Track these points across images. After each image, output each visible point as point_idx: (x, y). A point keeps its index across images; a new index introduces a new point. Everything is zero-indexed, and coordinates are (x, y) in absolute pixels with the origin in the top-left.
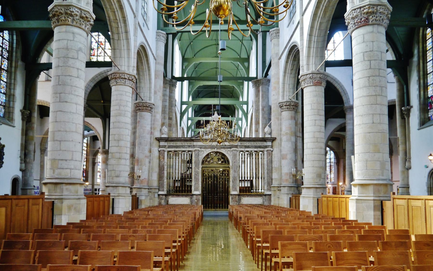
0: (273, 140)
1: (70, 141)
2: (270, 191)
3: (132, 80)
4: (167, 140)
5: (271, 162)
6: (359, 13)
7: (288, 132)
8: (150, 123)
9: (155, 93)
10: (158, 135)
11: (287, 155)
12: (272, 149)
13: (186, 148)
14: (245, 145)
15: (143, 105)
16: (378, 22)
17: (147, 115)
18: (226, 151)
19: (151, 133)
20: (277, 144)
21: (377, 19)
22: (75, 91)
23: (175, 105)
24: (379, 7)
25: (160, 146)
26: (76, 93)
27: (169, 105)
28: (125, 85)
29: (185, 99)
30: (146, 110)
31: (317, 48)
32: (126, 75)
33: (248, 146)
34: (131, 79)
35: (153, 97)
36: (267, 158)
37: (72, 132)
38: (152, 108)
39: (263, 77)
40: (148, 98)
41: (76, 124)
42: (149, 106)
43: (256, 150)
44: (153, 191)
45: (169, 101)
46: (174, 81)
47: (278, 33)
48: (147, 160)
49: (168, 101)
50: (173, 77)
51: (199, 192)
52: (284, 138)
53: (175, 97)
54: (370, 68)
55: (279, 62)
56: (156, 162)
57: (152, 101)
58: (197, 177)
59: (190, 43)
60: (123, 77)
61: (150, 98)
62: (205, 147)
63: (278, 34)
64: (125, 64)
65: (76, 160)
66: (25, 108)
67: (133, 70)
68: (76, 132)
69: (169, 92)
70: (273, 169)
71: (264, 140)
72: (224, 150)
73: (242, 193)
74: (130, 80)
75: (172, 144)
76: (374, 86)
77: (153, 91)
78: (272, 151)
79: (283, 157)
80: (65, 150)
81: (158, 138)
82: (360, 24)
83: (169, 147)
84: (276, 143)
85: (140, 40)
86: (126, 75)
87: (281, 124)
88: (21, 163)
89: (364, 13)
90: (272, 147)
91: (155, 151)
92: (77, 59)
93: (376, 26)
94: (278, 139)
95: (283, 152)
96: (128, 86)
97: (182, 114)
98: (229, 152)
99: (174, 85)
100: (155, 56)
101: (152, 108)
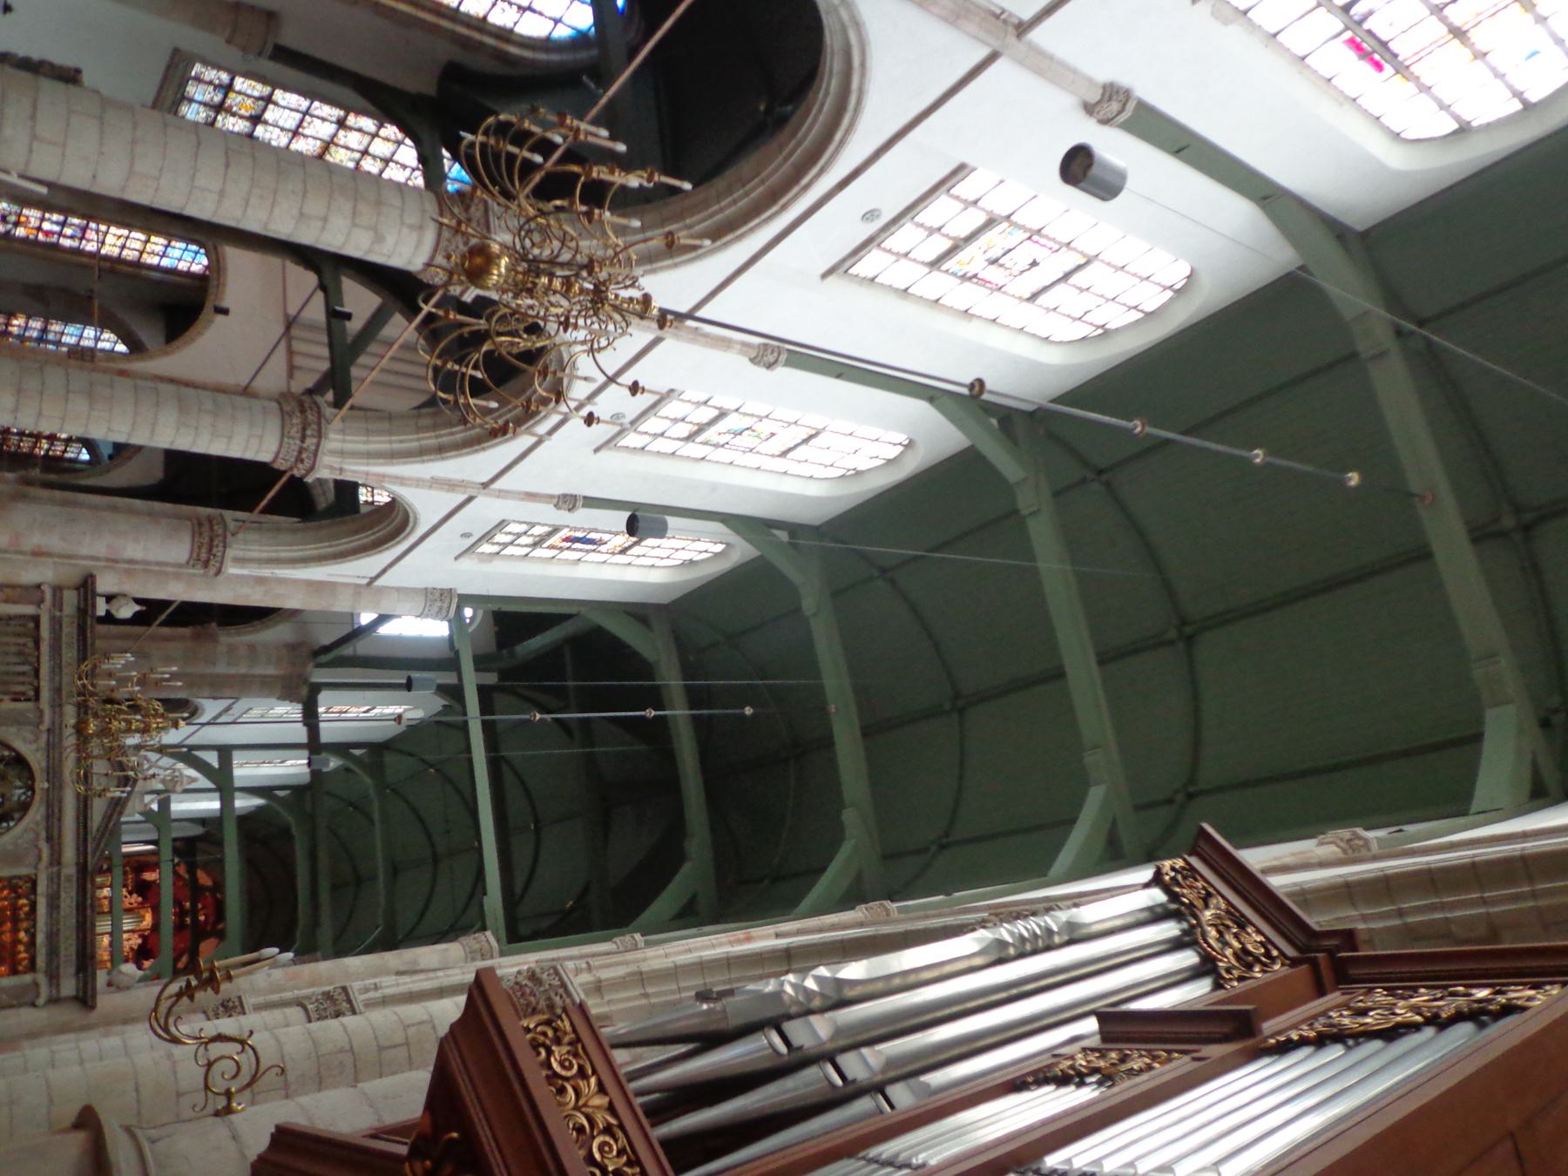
1: (101, 144)
3: (299, 460)
4: (84, 611)
6: (547, 987)
8: (151, 556)
9: (261, 581)
10: (105, 584)
13: (52, 680)
14: (63, 895)
15: (218, 536)
18: (37, 824)
19: (112, 562)
22: (262, 197)
23: (215, 695)
25: (58, 590)
26: (253, 201)
27: (218, 676)
28: (283, 436)
30: (196, 548)
32: (315, 441)
33: (58, 907)
34: (304, 456)
35: (245, 572)
37: (132, 164)
38: (206, 564)
40: (241, 554)
41: (158, 179)
42: (215, 556)
43: (40, 938)
45: (233, 676)
46: (304, 691)
49: (233, 671)
50: (316, 689)
53: (248, 696)
59: (432, 766)
60: (309, 432)
61: (240, 561)
62: (53, 748)
63: (479, 956)
64: (350, 442)
65: (31, 151)
67: (331, 468)
68: (131, 173)
69: (265, 676)
72: (38, 817)
74: (300, 452)
76: (319, 1073)
77: (266, 572)
78: (33, 1005)
80: (68, 125)
81: (93, 583)
82: (519, 994)
83: (56, 624)
84: (69, 1013)
85: (426, 505)
86: (315, 441)
89: (549, 999)
92: (354, 225)
96: (281, 446)
98: (31, 835)
99: (287, 695)
101: (206, 564)
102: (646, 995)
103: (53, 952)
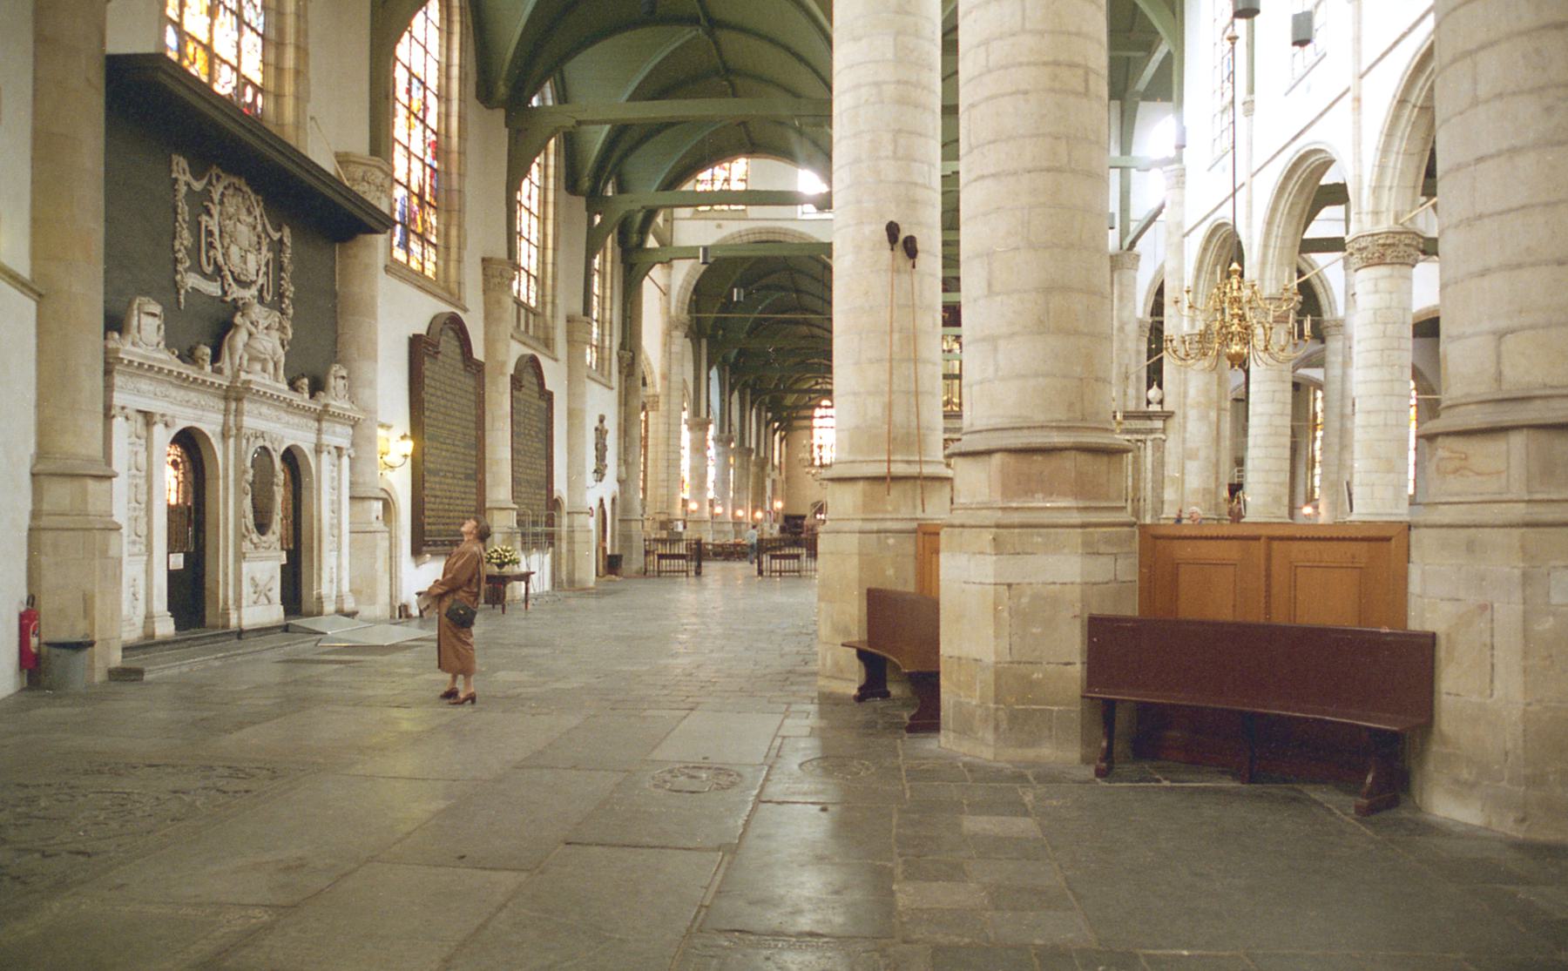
0: (1167, 416)
5: (1162, 464)
7: (1202, 399)
11: (1198, 449)
12: (1163, 437)
16: (1399, 261)
20: (1177, 425)
21: (1400, 255)
24: (1403, 236)
31: (1282, 248)
36: (1153, 455)
39: (1121, 248)
47: (1183, 175)
52: (1193, 414)
54: (1384, 336)
55: (1182, 242)
66: (623, 346)
70: (1166, 480)
71: (1149, 416)
78: (1164, 441)
79: (1188, 455)
84: (1173, 423)
87: (1185, 382)
88: (619, 466)
90: (1164, 431)
93: (1398, 266)
94: (1176, 411)
95: (1190, 445)
102: (1391, 188)
103: (1137, 431)
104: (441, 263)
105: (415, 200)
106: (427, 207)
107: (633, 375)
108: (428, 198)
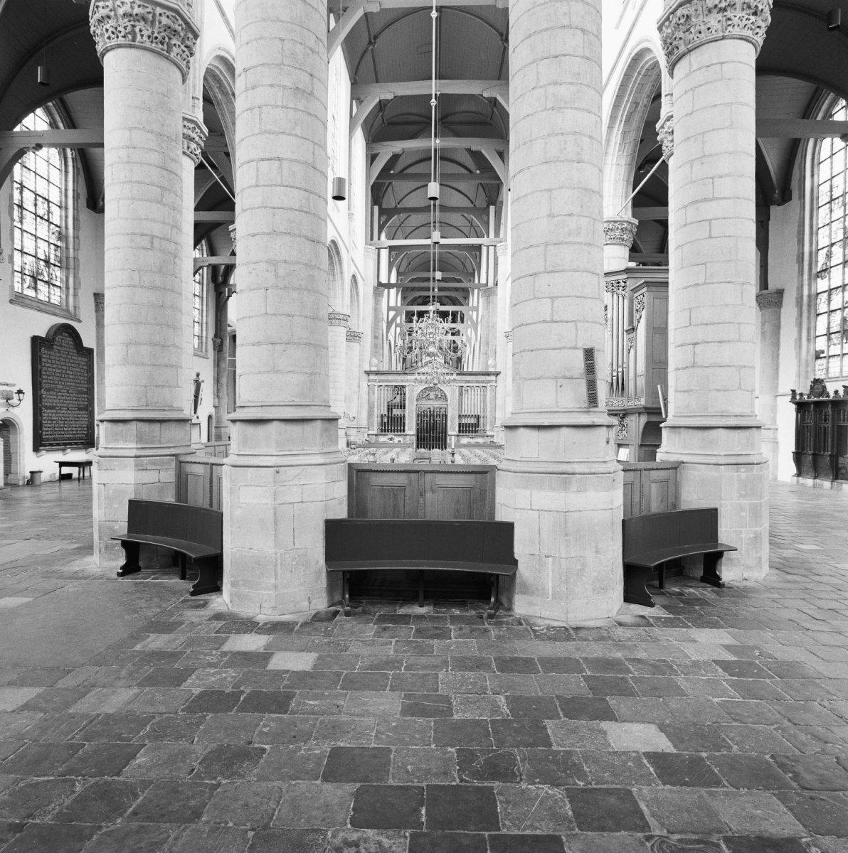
0: (497, 374)
2: (493, 431)
4: (377, 373)
9: (364, 320)
10: (367, 369)
17: (355, 345)
29: (392, 304)
40: (356, 327)
43: (477, 385)
44: (363, 430)
48: (356, 397)
50: (380, 284)
51: (413, 432)
56: (365, 397)
57: (361, 330)
58: (411, 415)
66: (216, 336)
67: (347, 309)
70: (497, 407)
71: (488, 374)
73: (461, 434)
75: (382, 377)
77: (361, 317)
83: (380, 381)
85: (353, 270)
88: (214, 399)
91: (364, 384)
97: (389, 324)
100: (363, 276)
103: (482, 382)
104: (64, 296)
105: (42, 263)
106: (52, 266)
107: (222, 351)
108: (52, 261)
